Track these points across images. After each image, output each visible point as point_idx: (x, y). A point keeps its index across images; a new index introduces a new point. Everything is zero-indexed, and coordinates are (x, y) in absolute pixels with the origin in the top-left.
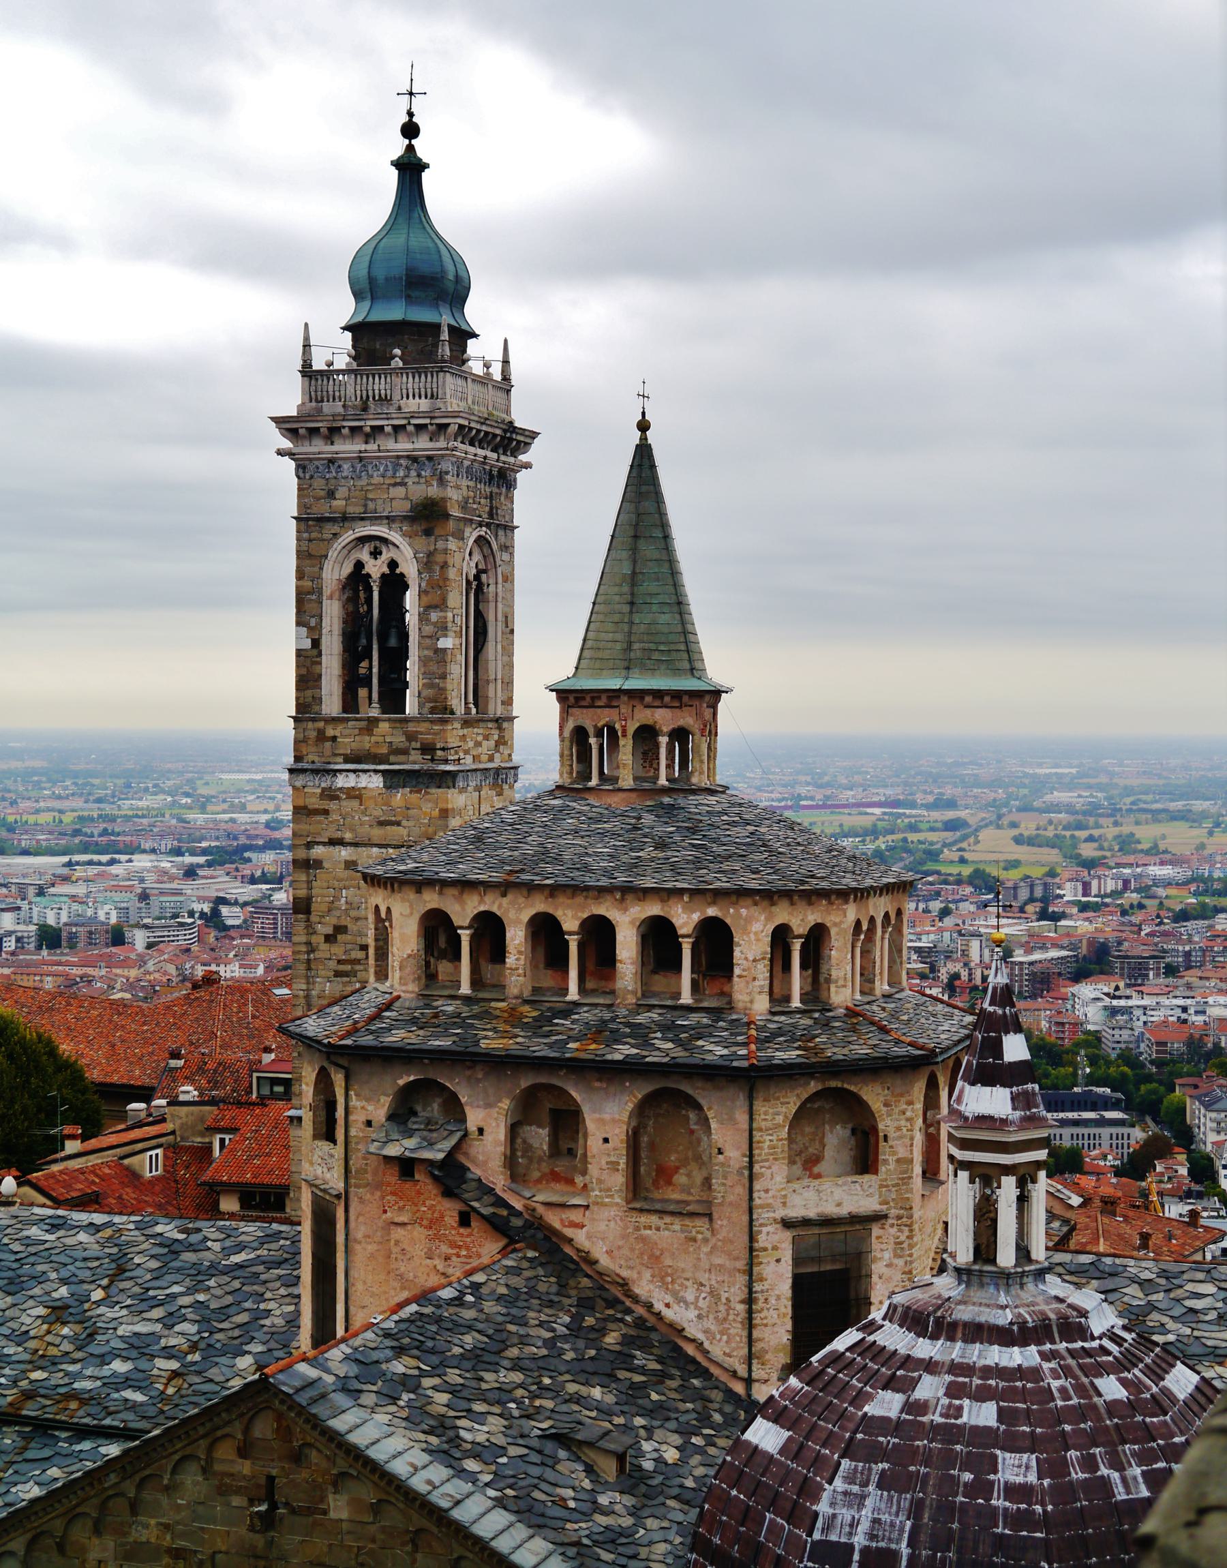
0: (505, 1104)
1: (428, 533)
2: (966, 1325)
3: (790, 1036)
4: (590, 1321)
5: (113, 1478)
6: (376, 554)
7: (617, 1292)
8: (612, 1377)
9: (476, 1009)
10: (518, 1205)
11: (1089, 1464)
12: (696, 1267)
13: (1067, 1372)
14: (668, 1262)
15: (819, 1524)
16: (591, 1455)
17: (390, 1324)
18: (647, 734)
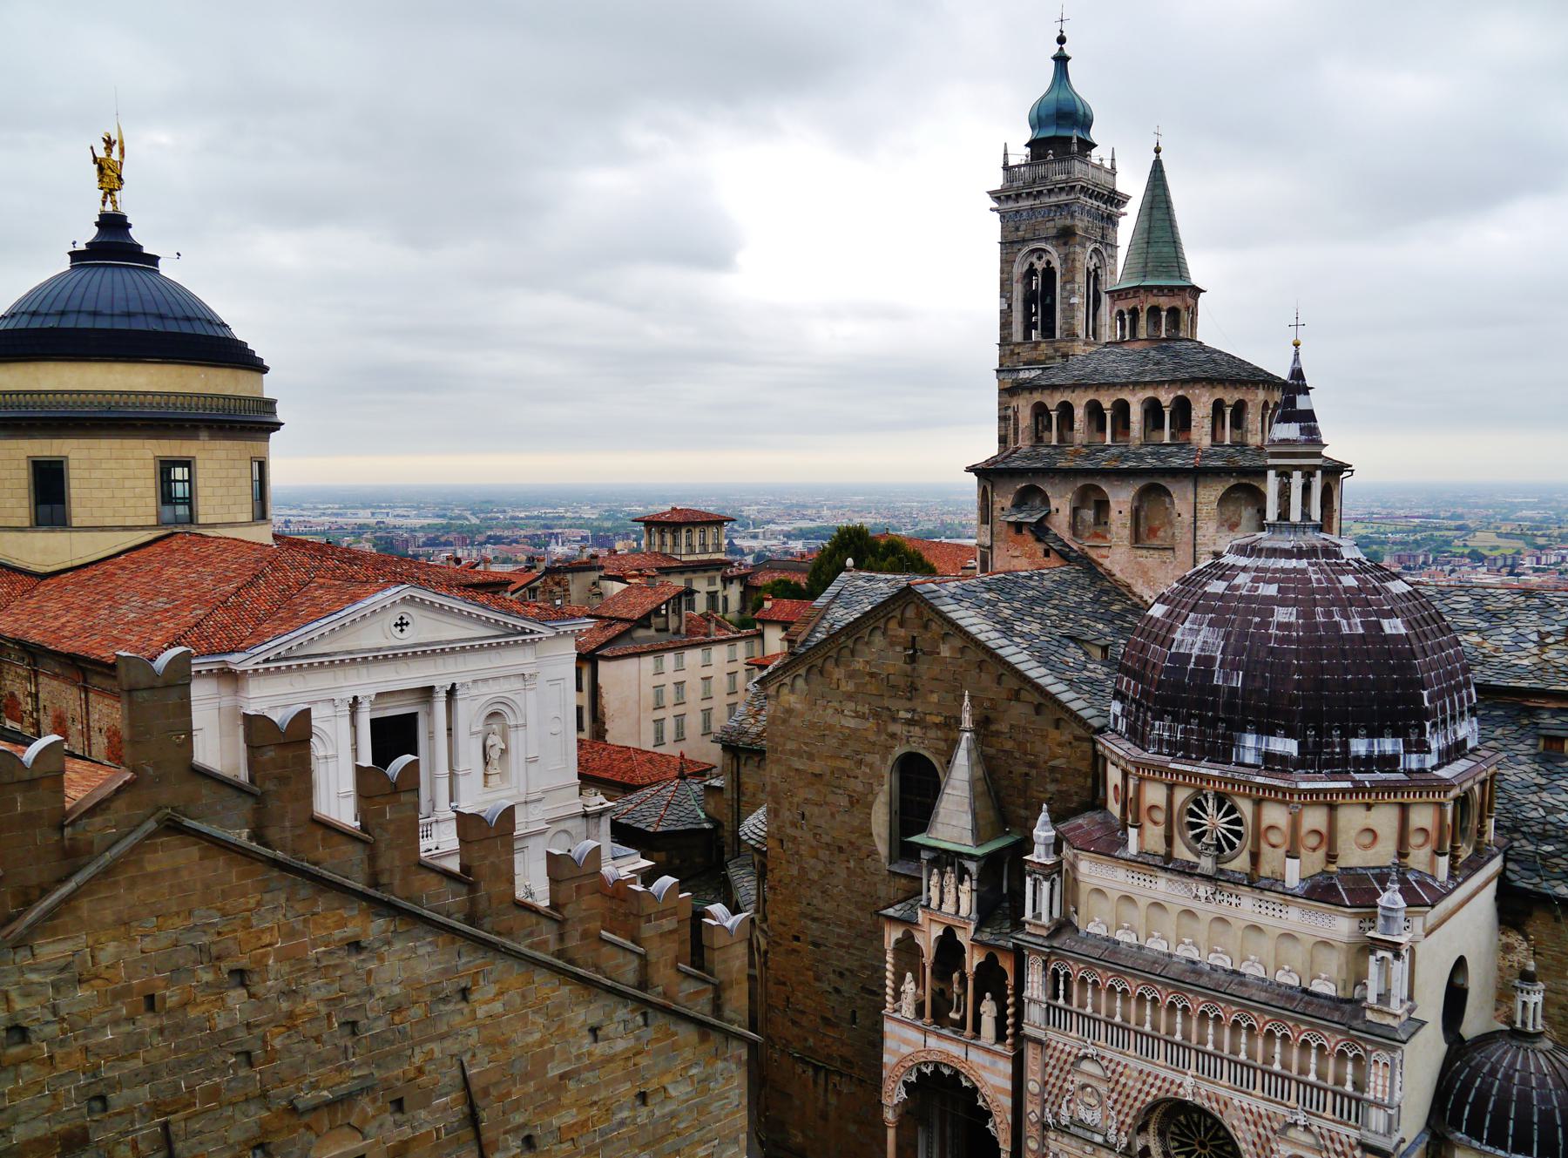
0: (1070, 496)
1: (1065, 244)
2: (1268, 549)
3: (1221, 456)
4: (1105, 598)
5: (843, 638)
6: (1040, 258)
7: (1124, 590)
8: (1111, 622)
10: (1075, 548)
11: (1329, 614)
12: (1166, 577)
13: (1322, 571)
16: (1088, 647)
17: (987, 579)
18: (1154, 311)
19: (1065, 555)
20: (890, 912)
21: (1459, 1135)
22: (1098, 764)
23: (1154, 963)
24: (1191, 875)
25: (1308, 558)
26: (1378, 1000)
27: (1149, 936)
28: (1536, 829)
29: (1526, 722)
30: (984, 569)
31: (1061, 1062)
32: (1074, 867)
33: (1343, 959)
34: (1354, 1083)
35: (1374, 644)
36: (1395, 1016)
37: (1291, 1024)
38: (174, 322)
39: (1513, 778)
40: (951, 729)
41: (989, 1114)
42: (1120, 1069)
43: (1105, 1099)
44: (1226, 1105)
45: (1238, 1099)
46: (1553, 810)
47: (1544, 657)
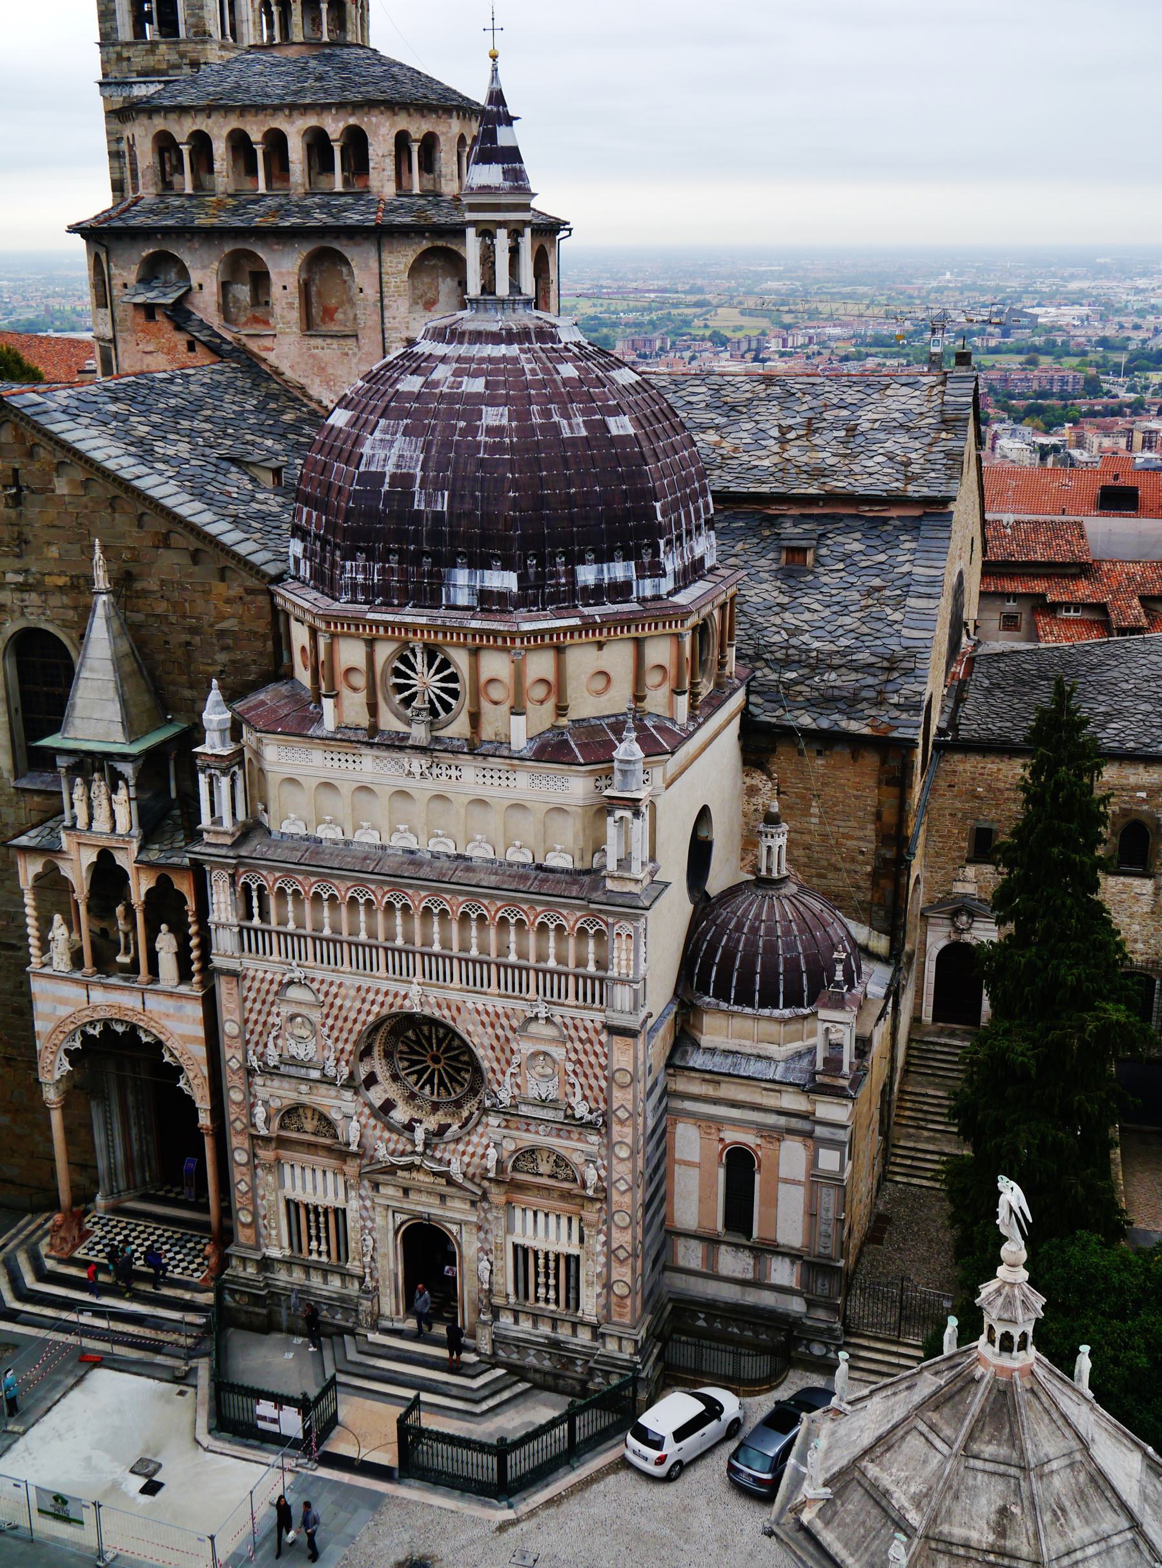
0: (215, 265)
2: (471, 333)
3: (409, 210)
4: (272, 405)
8: (283, 436)
9: (195, 202)
10: (229, 338)
11: (546, 414)
13: (537, 360)
14: (330, 371)
15: (364, 461)
16: (256, 471)
17: (111, 385)
19: (217, 349)
20: (23, 840)
21: (707, 999)
22: (278, 620)
23: (365, 859)
24: (401, 748)
25: (520, 343)
26: (619, 866)
27: (357, 827)
28: (778, 655)
29: (767, 533)
30: (107, 369)
31: (263, 994)
32: (258, 754)
33: (579, 825)
34: (597, 962)
35: (599, 448)
36: (637, 881)
37: (525, 907)
39: (755, 599)
40: (81, 593)
41: (180, 1070)
42: (334, 989)
43: (319, 1027)
44: (458, 1009)
45: (473, 1001)
46: (795, 632)
47: (785, 455)
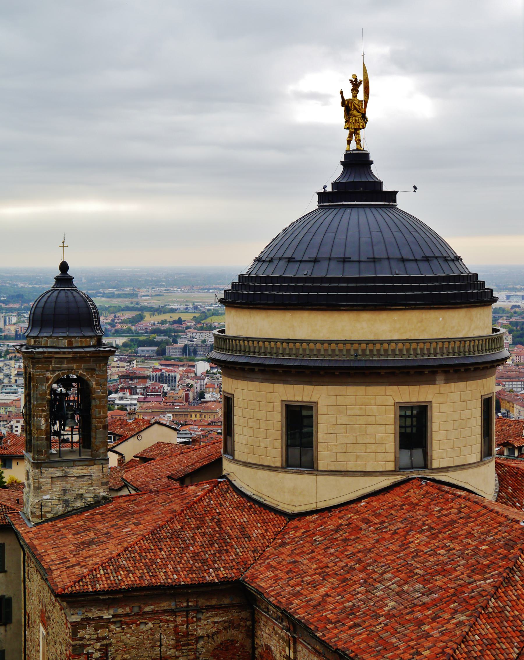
38: (413, 265)
